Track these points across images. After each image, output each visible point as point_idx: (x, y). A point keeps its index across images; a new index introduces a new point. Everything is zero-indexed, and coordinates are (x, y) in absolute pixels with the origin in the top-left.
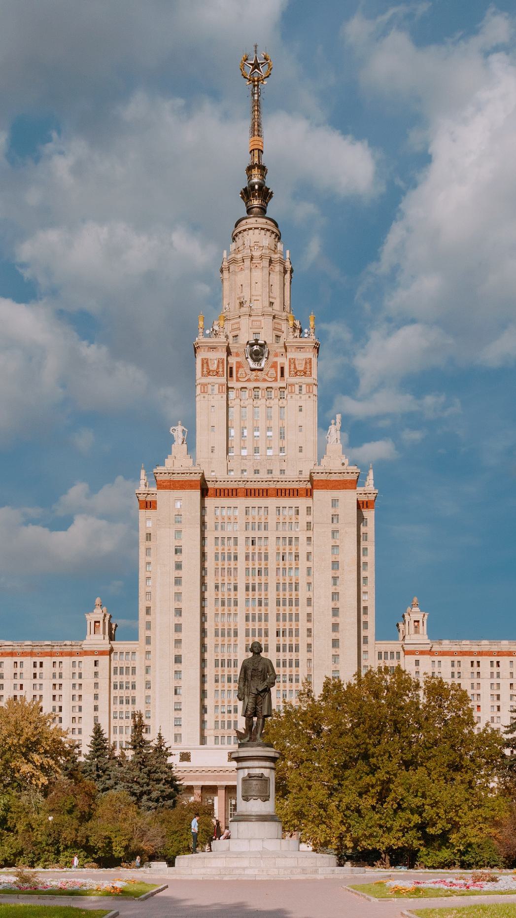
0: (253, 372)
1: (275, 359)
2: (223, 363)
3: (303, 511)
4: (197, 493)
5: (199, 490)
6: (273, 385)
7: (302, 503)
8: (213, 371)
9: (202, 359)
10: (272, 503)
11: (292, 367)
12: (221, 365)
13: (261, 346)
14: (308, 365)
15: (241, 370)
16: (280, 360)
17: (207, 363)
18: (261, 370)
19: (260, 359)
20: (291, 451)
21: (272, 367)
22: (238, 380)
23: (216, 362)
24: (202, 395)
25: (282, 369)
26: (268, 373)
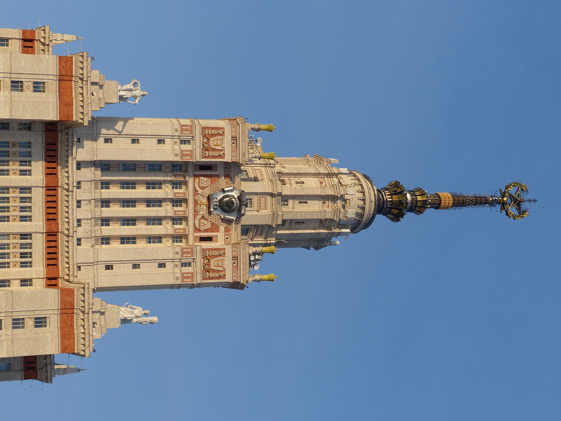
0: (205, 201)
1: (222, 228)
2: (220, 156)
3: (26, 273)
5: (58, 120)
6: (191, 229)
9: (224, 128)
11: (217, 253)
12: (215, 153)
13: (239, 210)
16: (220, 235)
21: (212, 224)
23: (220, 148)
24: (178, 127)
25: (209, 239)
26: (206, 219)
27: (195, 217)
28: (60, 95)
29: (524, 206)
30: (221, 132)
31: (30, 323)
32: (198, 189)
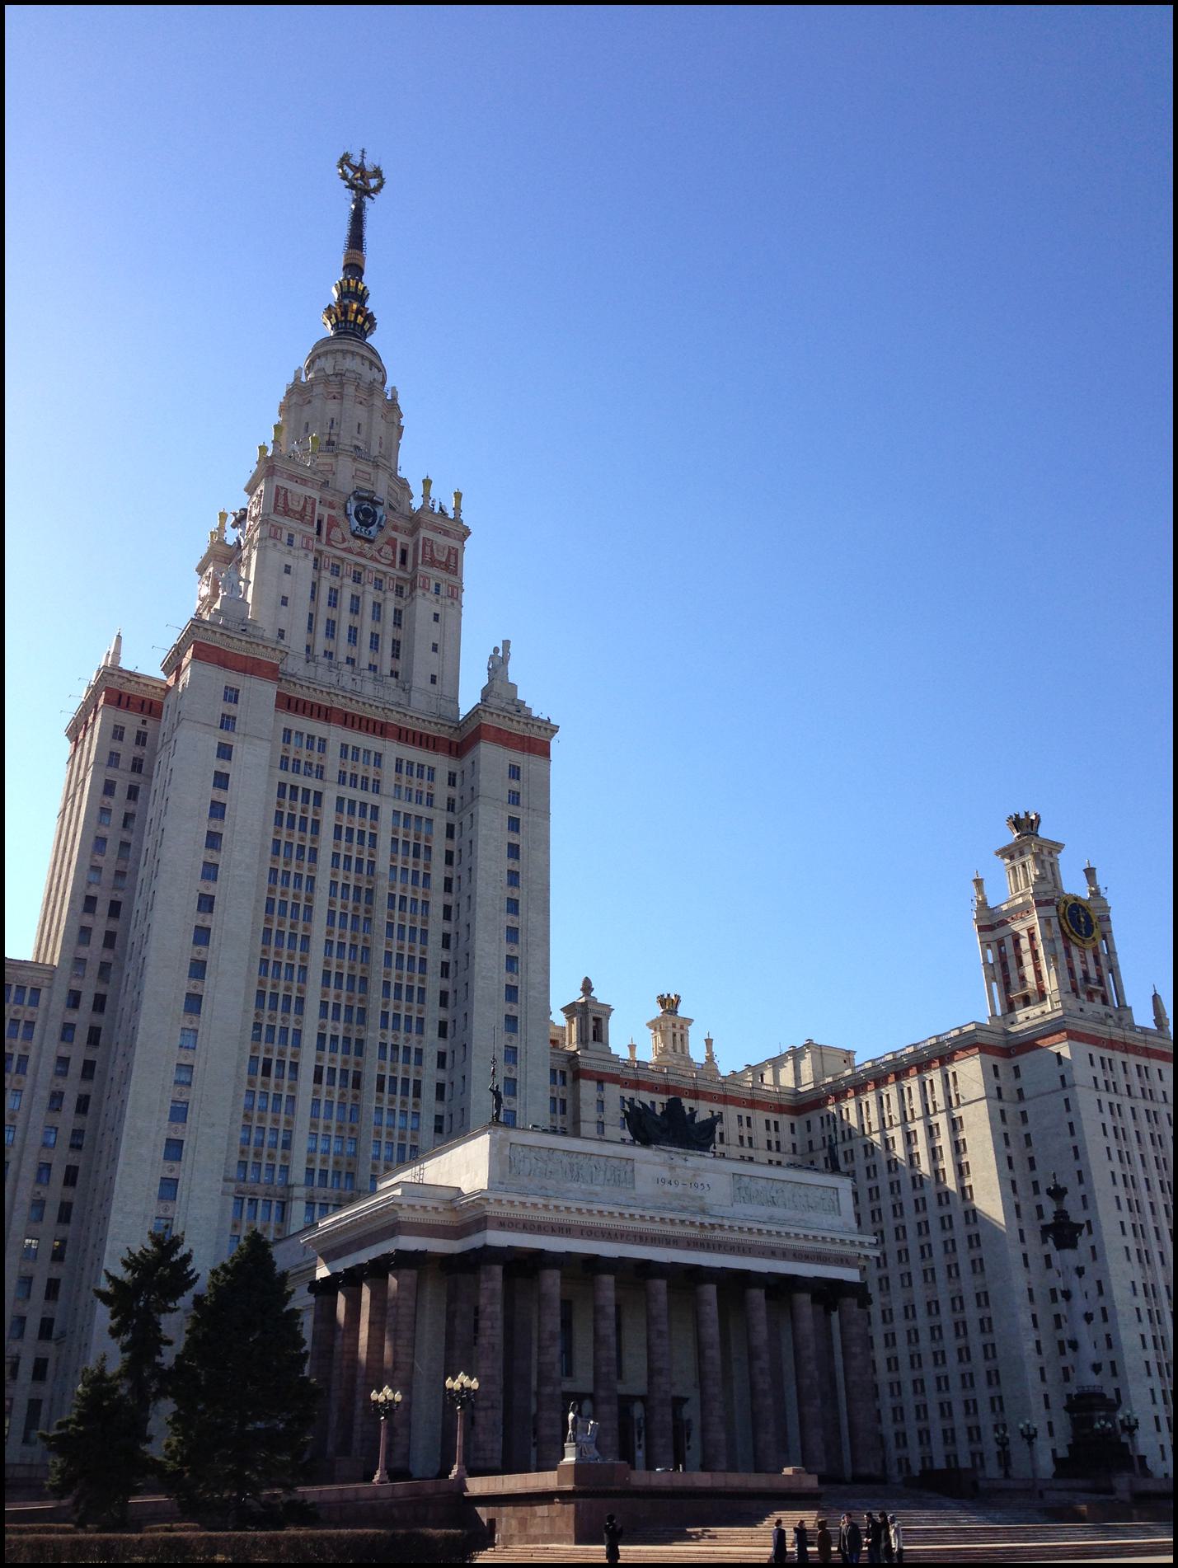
0: (358, 542)
1: (394, 534)
3: (442, 776)
4: (267, 691)
7: (441, 763)
8: (292, 510)
10: (392, 750)
11: (428, 549)
12: (309, 509)
14: (453, 557)
15: (336, 534)
17: (286, 493)
18: (370, 541)
19: (372, 524)
20: (420, 680)
22: (329, 543)
25: (404, 553)
27: (380, 562)
28: (244, 671)
29: (369, 168)
30: (283, 492)
31: (515, 785)
32: (345, 545)
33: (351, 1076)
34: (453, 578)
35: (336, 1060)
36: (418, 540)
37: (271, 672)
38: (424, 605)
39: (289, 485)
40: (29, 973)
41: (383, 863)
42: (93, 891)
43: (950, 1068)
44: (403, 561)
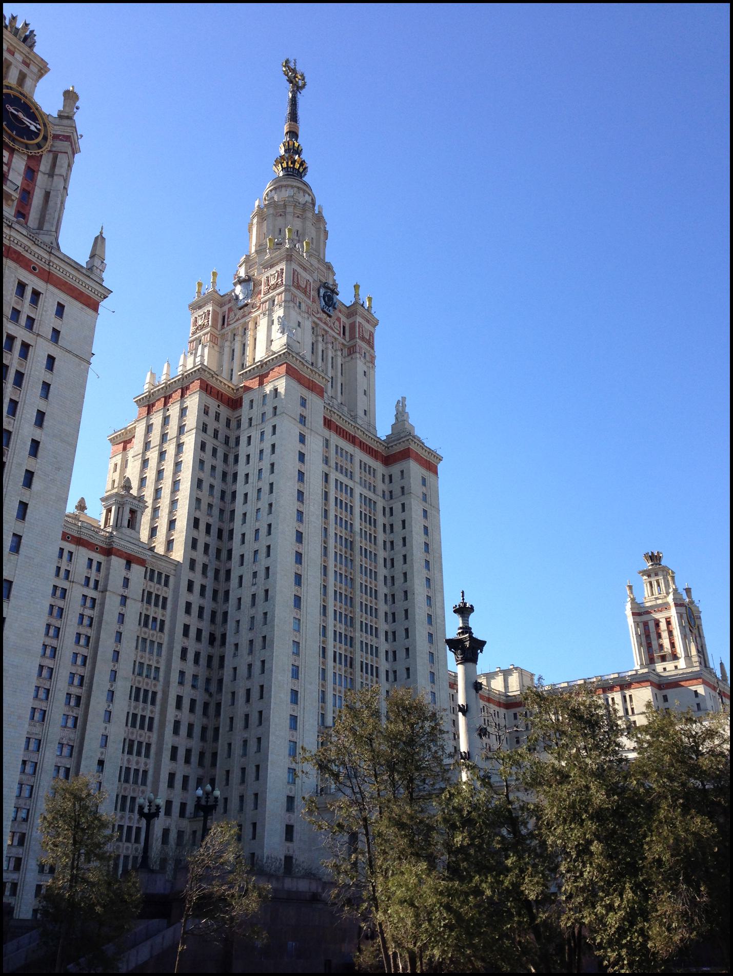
0: (325, 316)
1: (340, 315)
12: (308, 287)
18: (330, 316)
25: (344, 327)
32: (318, 316)
33: (349, 659)
34: (372, 351)
35: (342, 649)
36: (355, 322)
37: (320, 392)
38: (361, 366)
39: (299, 270)
40: (164, 564)
41: (357, 527)
42: (198, 514)
43: (627, 693)
44: (344, 334)
